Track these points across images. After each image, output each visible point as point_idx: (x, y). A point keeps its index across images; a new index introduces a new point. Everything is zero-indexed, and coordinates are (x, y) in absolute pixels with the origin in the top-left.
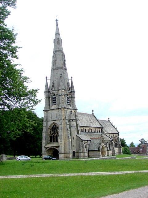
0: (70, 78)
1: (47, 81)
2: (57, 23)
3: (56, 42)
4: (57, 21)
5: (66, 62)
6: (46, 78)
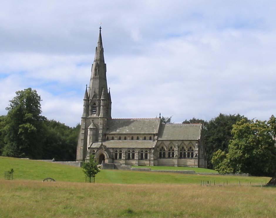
0: (108, 89)
1: (87, 88)
2: (100, 31)
3: (99, 51)
4: (100, 28)
5: (106, 73)
6: (87, 85)
